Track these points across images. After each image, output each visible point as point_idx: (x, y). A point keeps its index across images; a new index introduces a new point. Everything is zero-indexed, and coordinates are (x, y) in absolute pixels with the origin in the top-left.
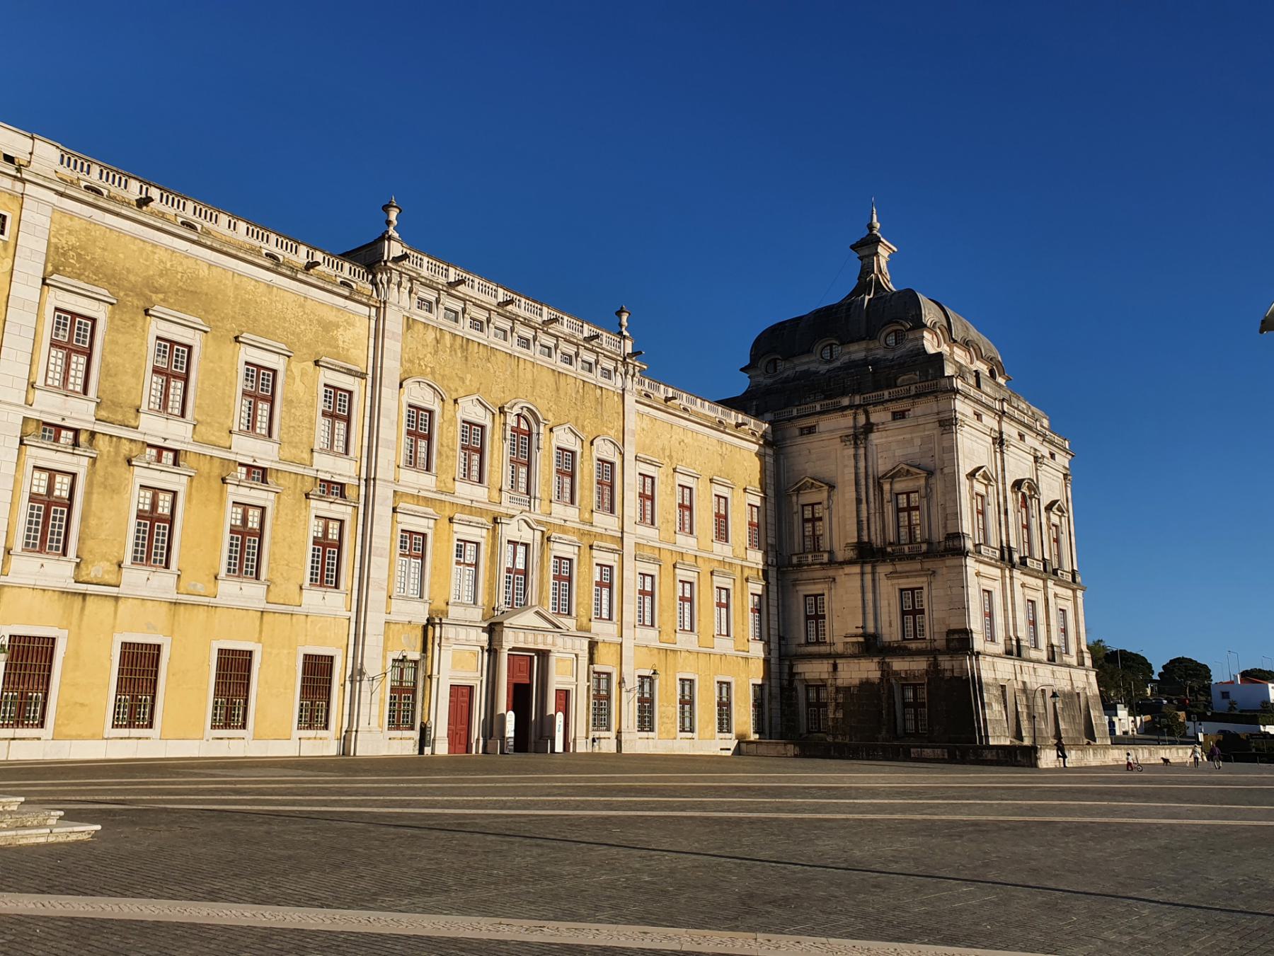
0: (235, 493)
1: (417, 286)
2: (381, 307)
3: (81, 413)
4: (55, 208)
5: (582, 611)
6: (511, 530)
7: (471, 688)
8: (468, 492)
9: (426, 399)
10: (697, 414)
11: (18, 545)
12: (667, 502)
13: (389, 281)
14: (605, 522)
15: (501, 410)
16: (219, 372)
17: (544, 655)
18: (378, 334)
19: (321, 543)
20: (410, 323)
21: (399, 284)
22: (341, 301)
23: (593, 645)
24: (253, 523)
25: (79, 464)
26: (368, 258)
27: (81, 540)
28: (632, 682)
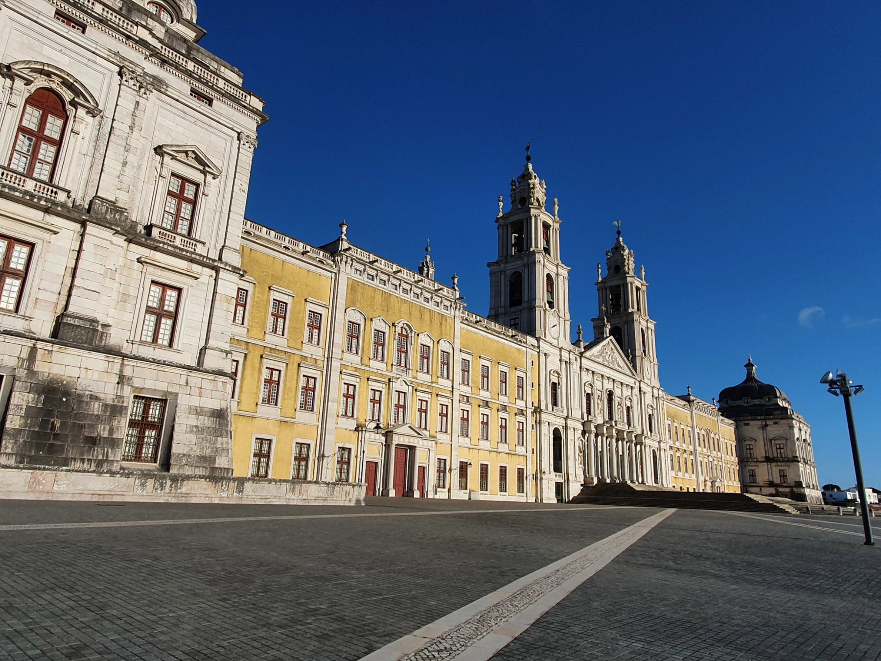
0: (267, 363)
1: (354, 263)
6: (397, 385)
7: (376, 463)
8: (375, 365)
9: (357, 318)
10: (492, 330)
12: (476, 373)
13: (341, 260)
14: (445, 383)
15: (393, 324)
17: (412, 448)
19: (306, 389)
21: (346, 262)
26: (332, 249)
28: (456, 465)
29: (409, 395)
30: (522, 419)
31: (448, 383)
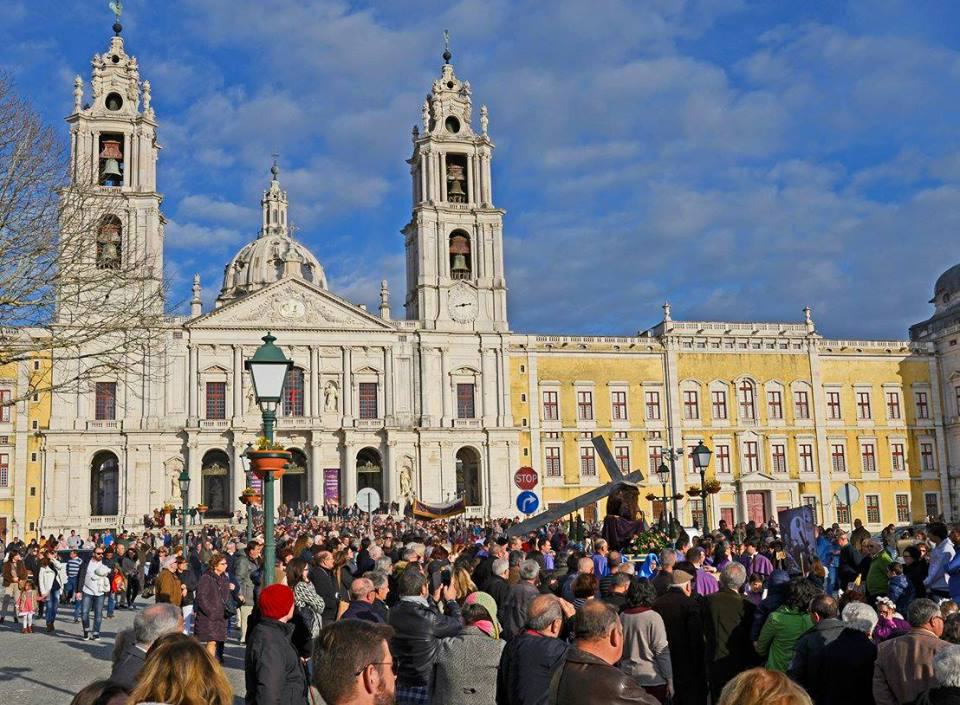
1: (681, 339)
2: (665, 354)
3: (556, 426)
4: (538, 357)
5: (793, 469)
7: (732, 509)
11: (546, 475)
12: (850, 402)
16: (604, 402)
17: (768, 492)
18: (666, 365)
20: (680, 356)
22: (648, 356)
23: (801, 485)
24: (625, 453)
25: (559, 444)
27: (565, 469)
29: (760, 446)
30: (932, 441)
31: (808, 423)
